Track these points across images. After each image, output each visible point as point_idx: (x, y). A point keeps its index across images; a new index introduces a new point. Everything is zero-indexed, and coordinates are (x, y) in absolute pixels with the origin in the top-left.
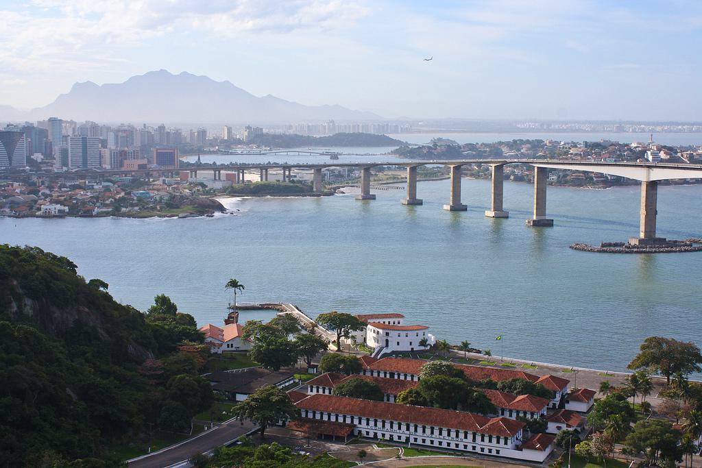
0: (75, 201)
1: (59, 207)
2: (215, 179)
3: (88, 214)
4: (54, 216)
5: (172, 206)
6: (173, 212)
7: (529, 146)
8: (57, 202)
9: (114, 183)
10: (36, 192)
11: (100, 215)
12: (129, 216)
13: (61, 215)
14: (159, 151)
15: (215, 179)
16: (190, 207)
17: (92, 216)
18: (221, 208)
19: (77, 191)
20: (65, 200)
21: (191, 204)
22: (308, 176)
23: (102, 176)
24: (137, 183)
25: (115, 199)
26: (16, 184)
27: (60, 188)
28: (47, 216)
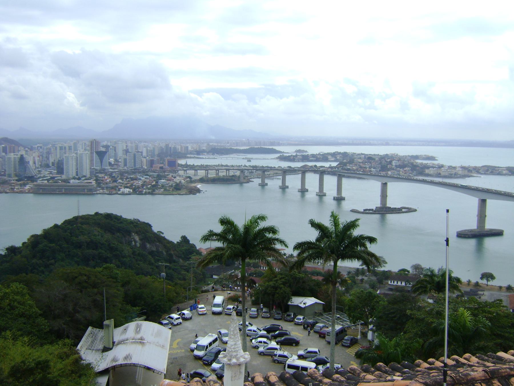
0: (134, 187)
1: (128, 190)
2: (195, 175)
3: (141, 193)
4: (127, 194)
5: (177, 189)
6: (178, 192)
7: (341, 155)
8: (127, 187)
9: (150, 176)
10: (115, 181)
11: (146, 194)
12: (159, 194)
13: (129, 194)
14: (169, 160)
15: (195, 175)
16: (185, 190)
17: (142, 194)
18: (199, 191)
19: (135, 181)
20: (130, 186)
21: (186, 188)
22: (238, 173)
23: (145, 173)
24: (159, 177)
25: (152, 185)
26: (106, 177)
27: (126, 179)
28: (123, 194)
